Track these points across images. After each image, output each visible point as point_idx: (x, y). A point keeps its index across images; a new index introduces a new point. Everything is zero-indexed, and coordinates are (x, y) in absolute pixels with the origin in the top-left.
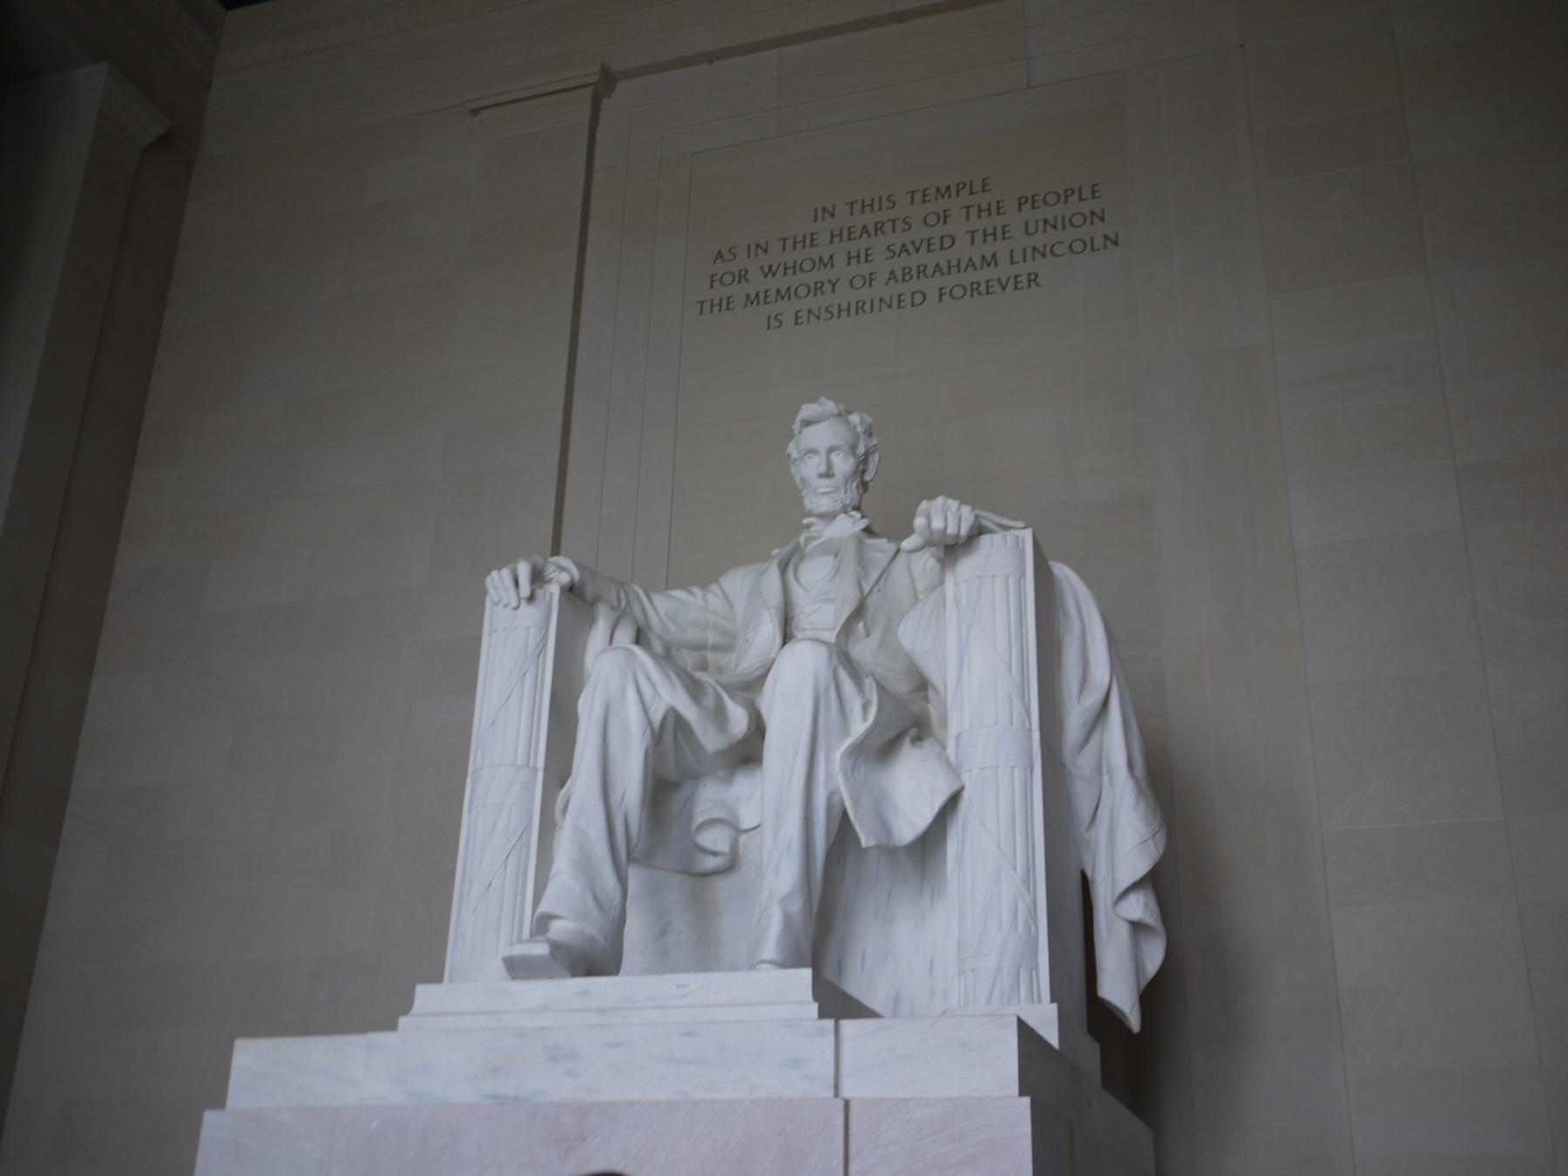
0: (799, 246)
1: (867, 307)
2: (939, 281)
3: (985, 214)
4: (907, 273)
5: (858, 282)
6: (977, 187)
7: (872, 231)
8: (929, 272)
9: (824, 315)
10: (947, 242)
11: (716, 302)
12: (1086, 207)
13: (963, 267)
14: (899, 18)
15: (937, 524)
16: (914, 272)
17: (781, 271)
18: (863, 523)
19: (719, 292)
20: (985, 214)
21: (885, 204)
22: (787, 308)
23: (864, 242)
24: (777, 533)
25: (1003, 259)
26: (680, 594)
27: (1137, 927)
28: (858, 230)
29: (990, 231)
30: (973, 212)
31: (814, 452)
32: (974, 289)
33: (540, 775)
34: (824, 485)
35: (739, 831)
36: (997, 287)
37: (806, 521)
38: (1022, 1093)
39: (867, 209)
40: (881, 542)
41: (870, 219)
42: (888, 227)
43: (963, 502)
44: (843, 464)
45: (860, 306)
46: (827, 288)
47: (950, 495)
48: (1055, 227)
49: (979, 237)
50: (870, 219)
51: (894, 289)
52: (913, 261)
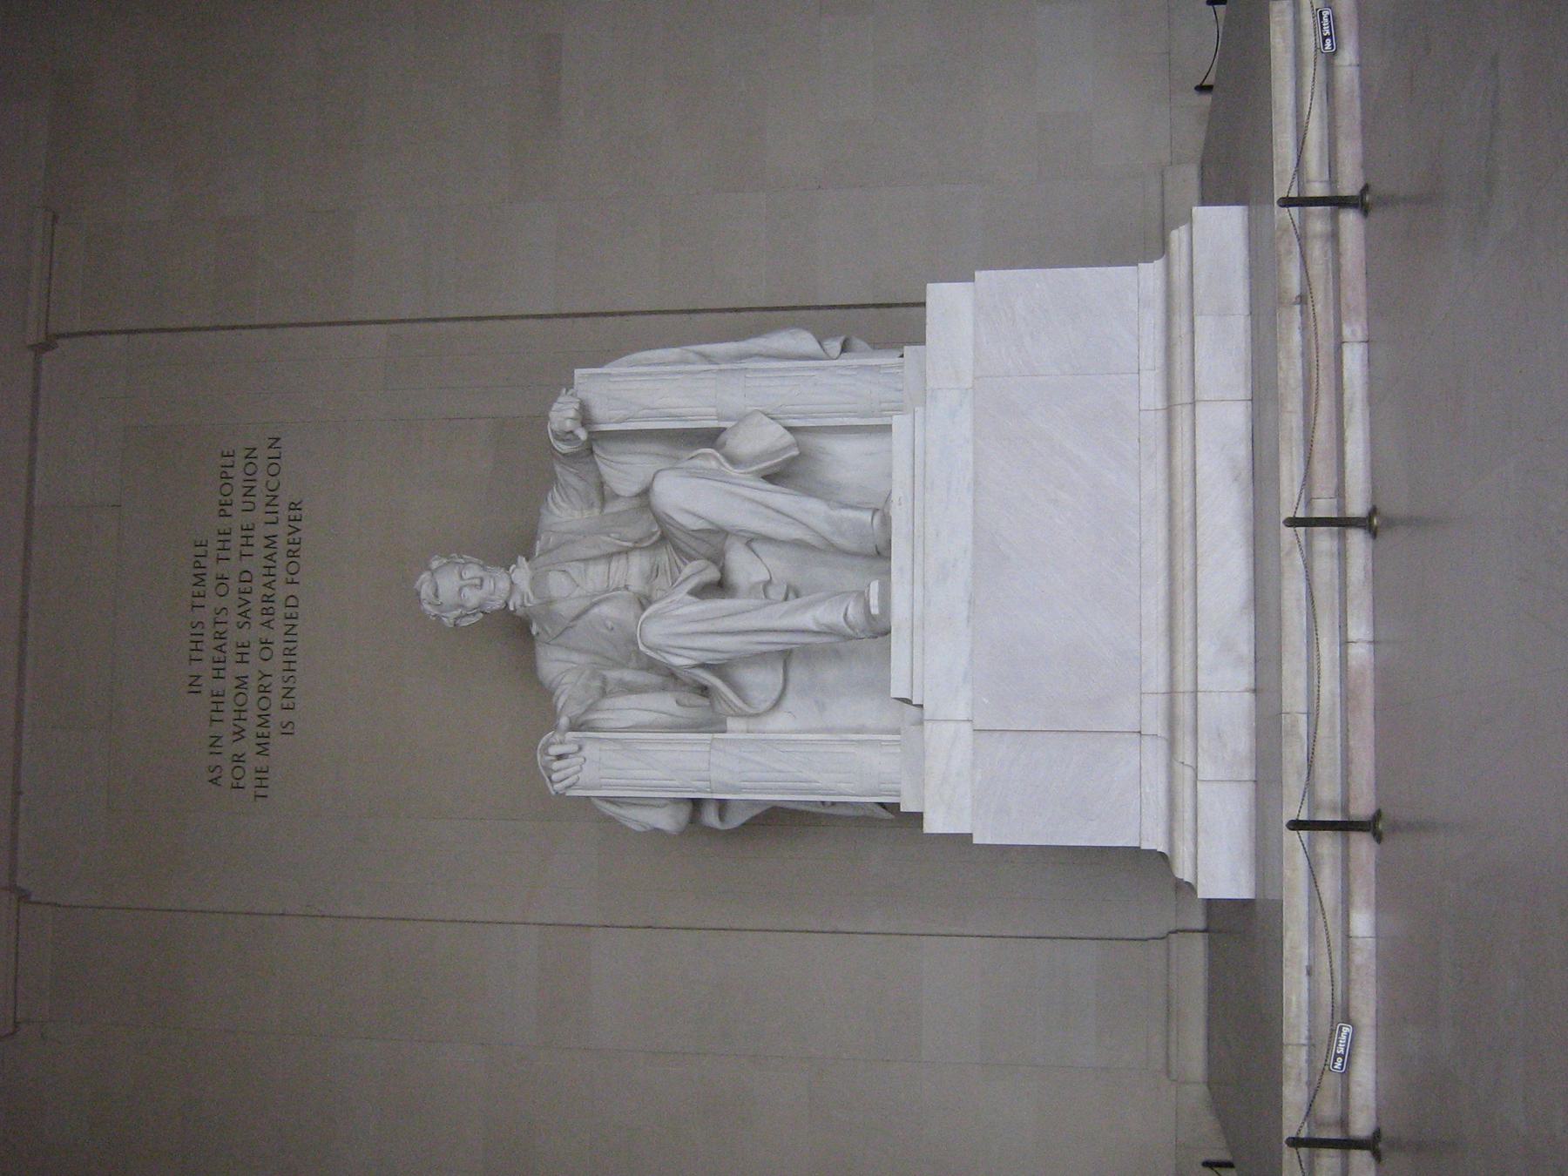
0: (221, 707)
1: (291, 645)
2: (279, 585)
3: (227, 545)
4: (265, 611)
5: (266, 654)
6: (200, 551)
9: (289, 684)
10: (246, 577)
12: (240, 461)
13: (270, 563)
14: (24, 616)
15: (572, 413)
18: (522, 560)
19: (249, 780)
20: (227, 545)
21: (198, 630)
22: (277, 716)
23: (230, 649)
24: (515, 632)
25: (271, 530)
26: (562, 699)
27: (844, 349)
28: (217, 654)
31: (461, 590)
32: (292, 554)
33: (717, 736)
34: (489, 585)
35: (768, 583)
36: (296, 536)
38: (971, 279)
40: (538, 545)
41: (209, 642)
42: (221, 628)
44: (472, 572)
45: (290, 652)
49: (246, 550)
50: (209, 642)
51: (279, 623)
52: (256, 605)
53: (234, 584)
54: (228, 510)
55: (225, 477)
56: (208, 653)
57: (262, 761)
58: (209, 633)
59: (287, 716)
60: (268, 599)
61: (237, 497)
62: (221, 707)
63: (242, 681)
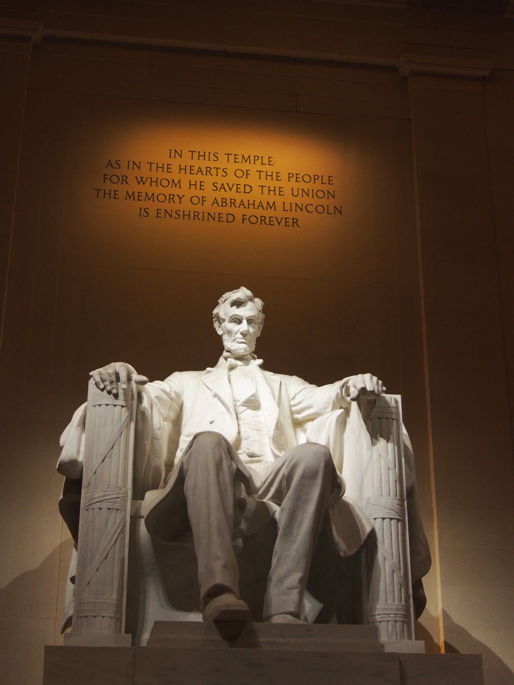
0: (160, 170)
2: (242, 210)
3: (269, 178)
4: (224, 201)
6: (266, 161)
7: (204, 173)
8: (237, 204)
10: (248, 189)
11: (107, 192)
12: (325, 188)
13: (256, 207)
16: (228, 202)
17: (148, 183)
18: (260, 361)
19: (109, 186)
20: (269, 178)
23: (199, 177)
25: (279, 206)
28: (196, 169)
29: (272, 188)
30: (263, 175)
37: (225, 354)
39: (202, 158)
42: (214, 171)
43: (379, 378)
46: (177, 199)
47: (373, 374)
48: (308, 195)
49: (266, 190)
50: (203, 164)
52: (229, 195)
53: (243, 181)
54: (293, 179)
55: (316, 177)
56: (197, 163)
57: (122, 194)
58: (212, 164)
59: (153, 213)
60: (233, 202)
61: (302, 185)
62: (160, 170)
63: (178, 184)
